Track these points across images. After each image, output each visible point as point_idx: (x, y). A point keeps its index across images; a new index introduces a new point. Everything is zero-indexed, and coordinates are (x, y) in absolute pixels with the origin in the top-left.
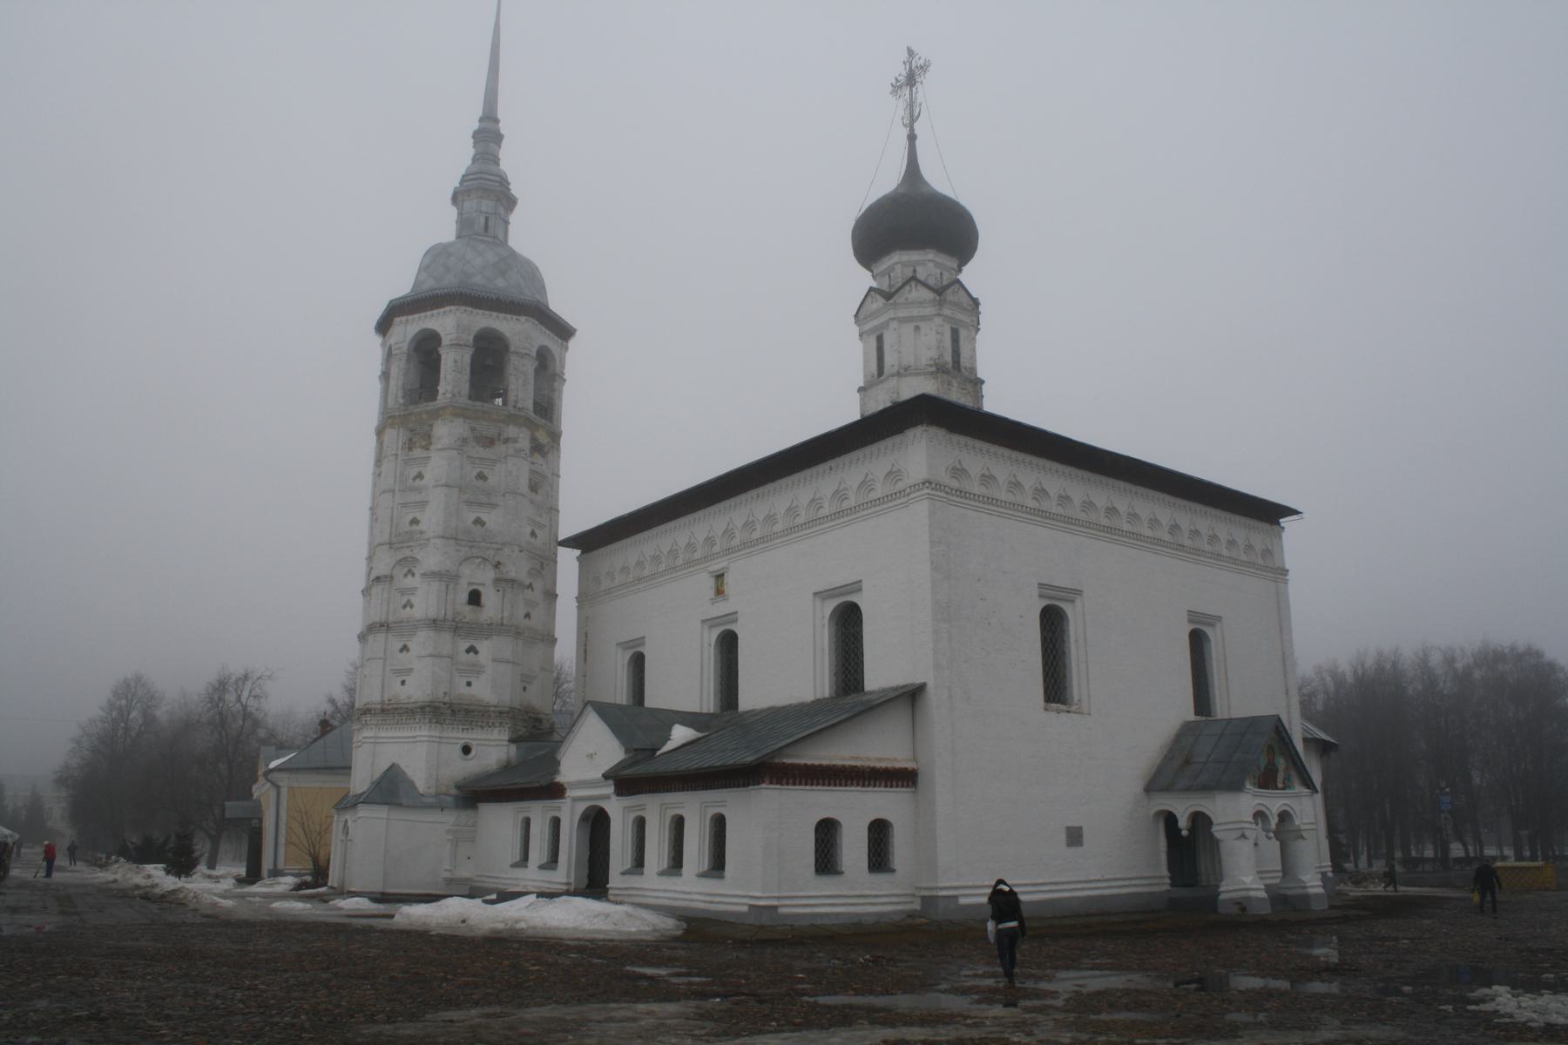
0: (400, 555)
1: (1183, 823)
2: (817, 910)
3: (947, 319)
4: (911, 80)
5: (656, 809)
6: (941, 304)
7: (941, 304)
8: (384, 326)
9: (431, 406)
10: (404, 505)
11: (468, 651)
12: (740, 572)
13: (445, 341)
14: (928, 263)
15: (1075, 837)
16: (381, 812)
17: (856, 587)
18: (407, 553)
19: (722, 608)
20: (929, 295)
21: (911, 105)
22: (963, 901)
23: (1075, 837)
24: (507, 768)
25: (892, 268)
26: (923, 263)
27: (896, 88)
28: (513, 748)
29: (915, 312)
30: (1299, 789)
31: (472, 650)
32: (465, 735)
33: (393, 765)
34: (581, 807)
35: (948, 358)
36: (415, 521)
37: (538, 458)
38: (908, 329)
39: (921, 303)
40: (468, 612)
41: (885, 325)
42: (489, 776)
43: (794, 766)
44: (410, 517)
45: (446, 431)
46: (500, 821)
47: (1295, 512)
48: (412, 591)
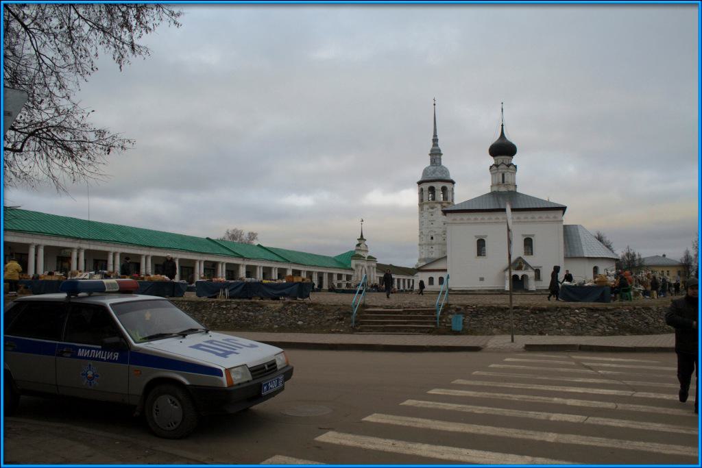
6: (498, 169)
7: (498, 169)
14: (501, 159)
15: (482, 279)
23: (482, 279)
30: (530, 270)
35: (501, 180)
45: (426, 207)
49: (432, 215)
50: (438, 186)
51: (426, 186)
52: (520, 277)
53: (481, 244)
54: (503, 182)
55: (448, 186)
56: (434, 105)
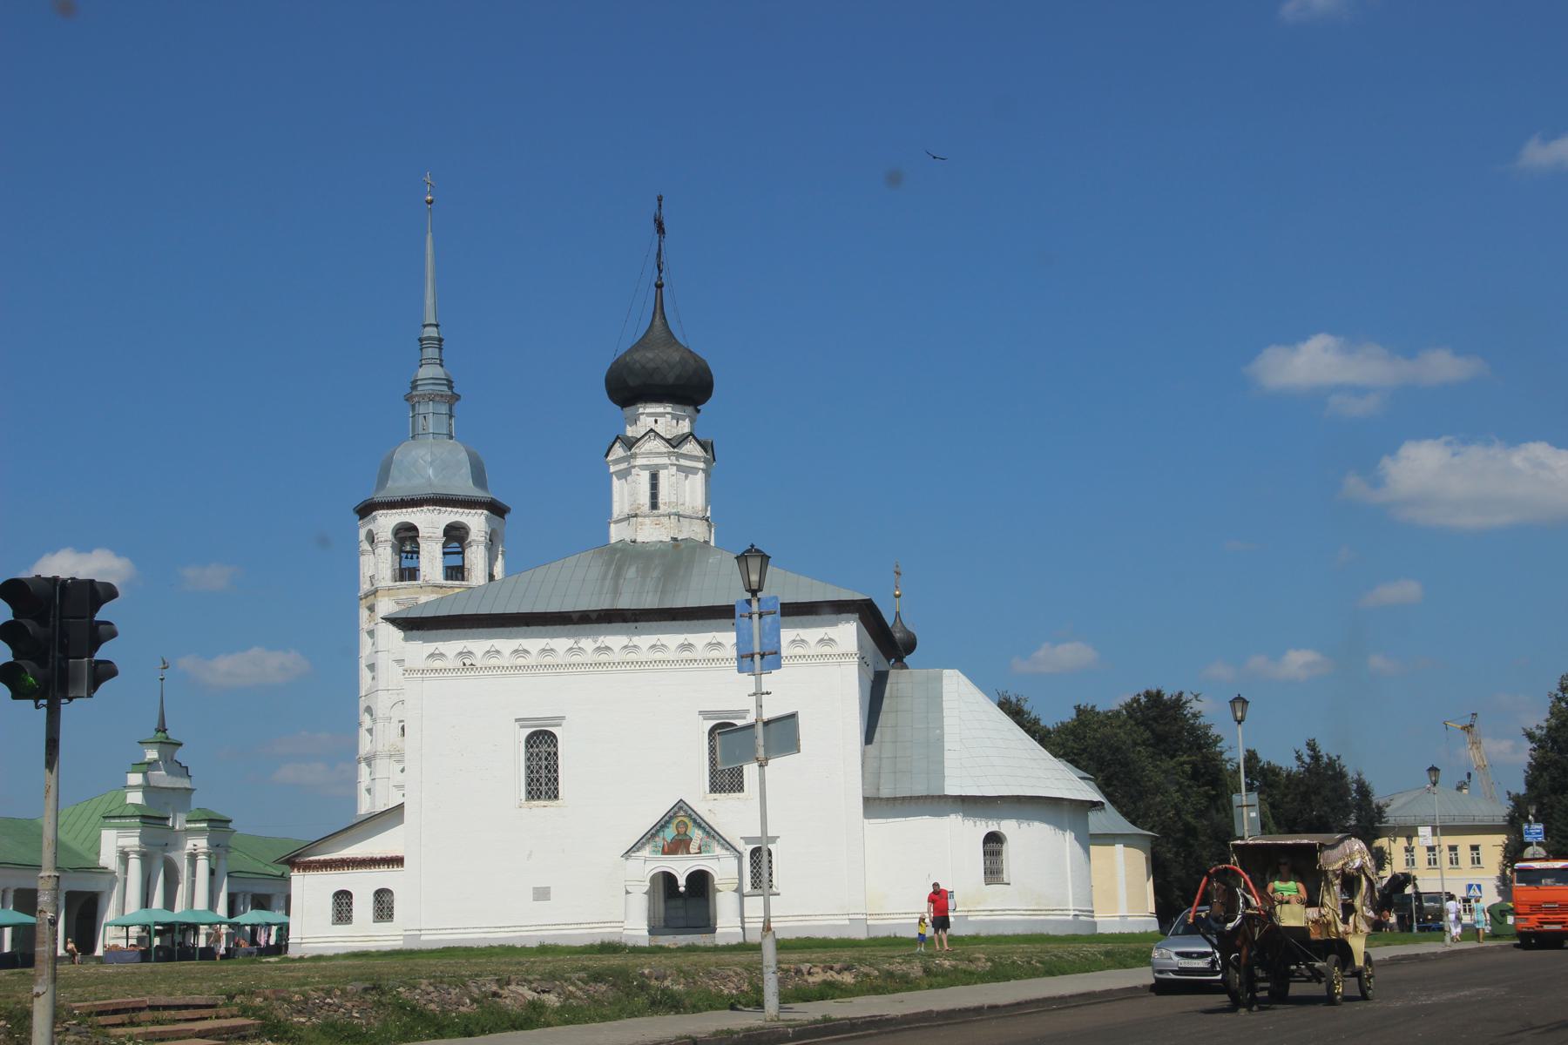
7: (634, 456)
15: (542, 894)
23: (542, 894)
29: (624, 466)
30: (718, 850)
35: (645, 499)
50: (430, 522)
52: (682, 882)
53: (542, 748)
54: (654, 505)
55: (477, 522)
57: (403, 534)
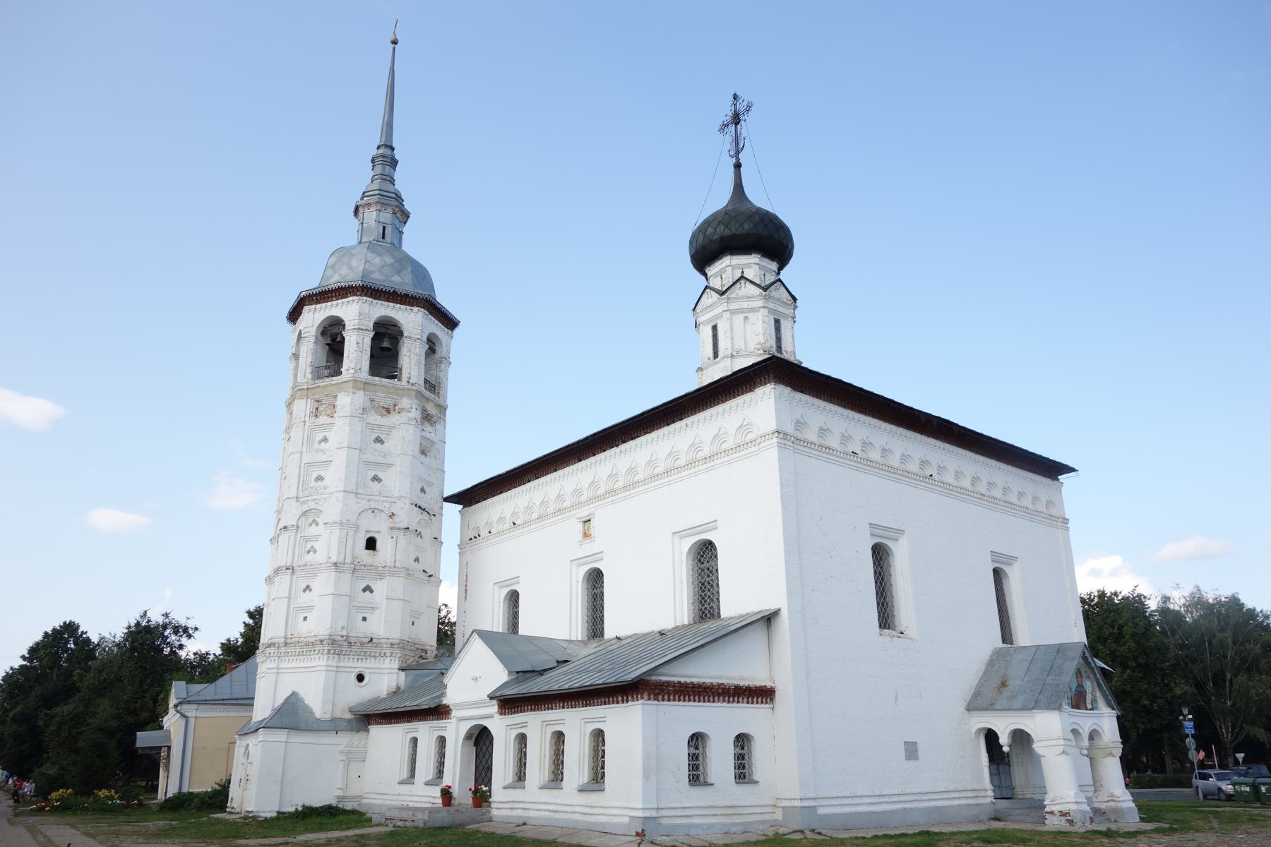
0: (305, 508)
1: (1004, 740)
2: (678, 821)
3: (771, 311)
4: (736, 119)
5: (537, 724)
6: (766, 298)
8: (294, 315)
9: (336, 379)
10: (310, 464)
11: (364, 590)
12: (603, 518)
13: (349, 325)
15: (911, 751)
16: (281, 736)
17: (712, 525)
18: (312, 505)
19: (589, 548)
20: (758, 291)
21: (736, 140)
22: (821, 811)
23: (911, 751)
24: (397, 692)
25: (723, 270)
26: (749, 265)
27: (725, 126)
28: (403, 674)
29: (745, 305)
31: (368, 589)
32: (360, 664)
33: (294, 694)
34: (465, 727)
36: (319, 478)
37: (428, 428)
38: (739, 318)
39: (749, 298)
40: (366, 555)
41: (719, 316)
42: (378, 700)
43: (668, 684)
44: (315, 475)
45: (347, 401)
46: (388, 741)
47: (1073, 470)
48: (316, 538)
49: (379, 440)
51: (357, 315)
56: (395, 42)
57: (382, 330)
